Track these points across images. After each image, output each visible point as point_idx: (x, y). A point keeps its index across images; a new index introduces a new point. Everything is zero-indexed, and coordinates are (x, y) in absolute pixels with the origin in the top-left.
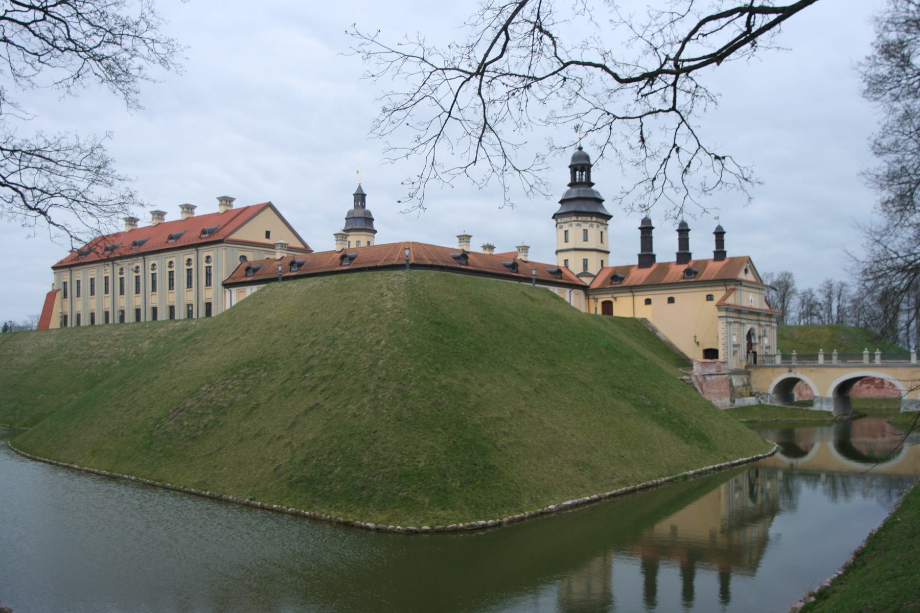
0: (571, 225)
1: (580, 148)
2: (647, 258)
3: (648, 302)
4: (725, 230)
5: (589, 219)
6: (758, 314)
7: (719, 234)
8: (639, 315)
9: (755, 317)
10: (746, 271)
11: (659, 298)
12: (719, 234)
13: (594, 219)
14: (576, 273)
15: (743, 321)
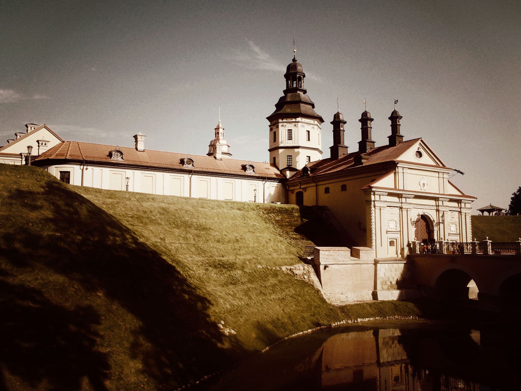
0: (278, 127)
1: (294, 60)
2: (334, 150)
3: (327, 190)
4: (400, 113)
5: (294, 120)
6: (436, 199)
7: (395, 118)
8: (321, 204)
9: (433, 202)
10: (419, 154)
11: (335, 187)
12: (395, 118)
13: (299, 119)
14: (280, 169)
15: (404, 206)
